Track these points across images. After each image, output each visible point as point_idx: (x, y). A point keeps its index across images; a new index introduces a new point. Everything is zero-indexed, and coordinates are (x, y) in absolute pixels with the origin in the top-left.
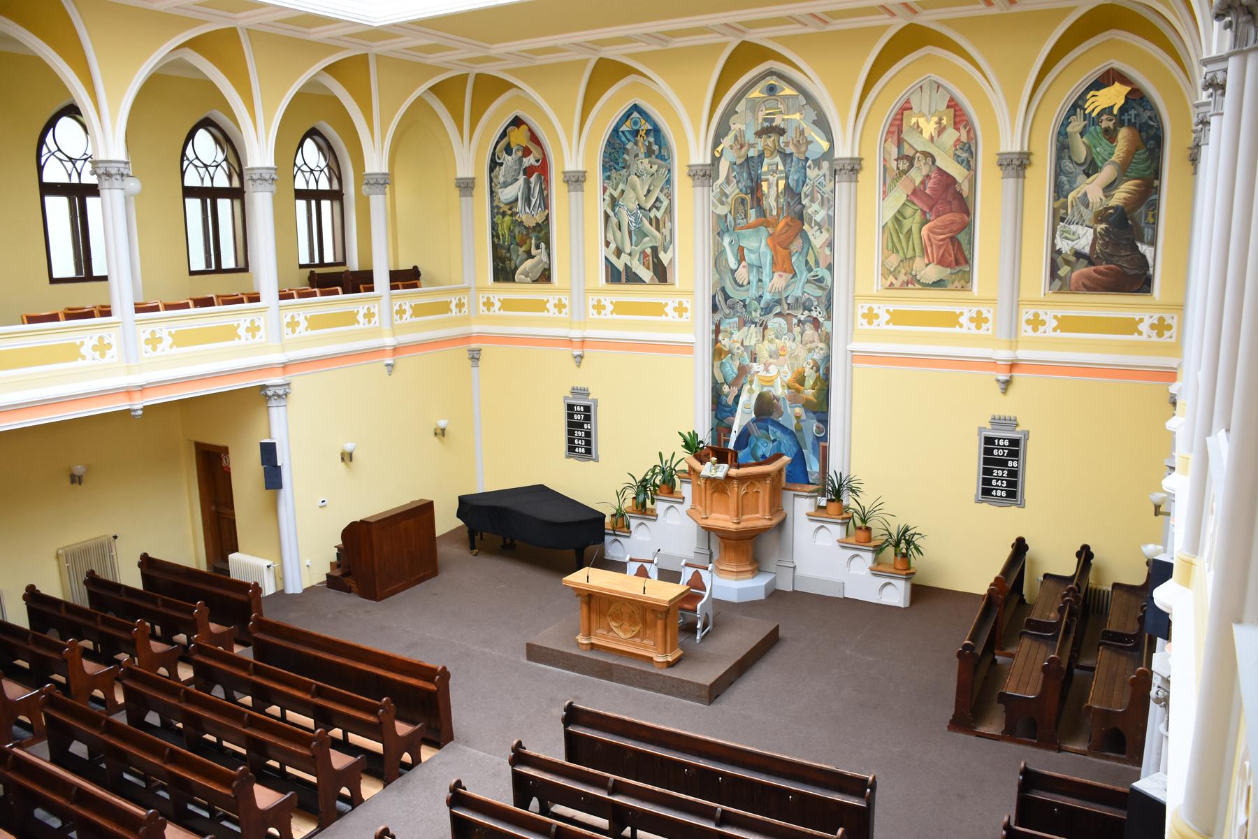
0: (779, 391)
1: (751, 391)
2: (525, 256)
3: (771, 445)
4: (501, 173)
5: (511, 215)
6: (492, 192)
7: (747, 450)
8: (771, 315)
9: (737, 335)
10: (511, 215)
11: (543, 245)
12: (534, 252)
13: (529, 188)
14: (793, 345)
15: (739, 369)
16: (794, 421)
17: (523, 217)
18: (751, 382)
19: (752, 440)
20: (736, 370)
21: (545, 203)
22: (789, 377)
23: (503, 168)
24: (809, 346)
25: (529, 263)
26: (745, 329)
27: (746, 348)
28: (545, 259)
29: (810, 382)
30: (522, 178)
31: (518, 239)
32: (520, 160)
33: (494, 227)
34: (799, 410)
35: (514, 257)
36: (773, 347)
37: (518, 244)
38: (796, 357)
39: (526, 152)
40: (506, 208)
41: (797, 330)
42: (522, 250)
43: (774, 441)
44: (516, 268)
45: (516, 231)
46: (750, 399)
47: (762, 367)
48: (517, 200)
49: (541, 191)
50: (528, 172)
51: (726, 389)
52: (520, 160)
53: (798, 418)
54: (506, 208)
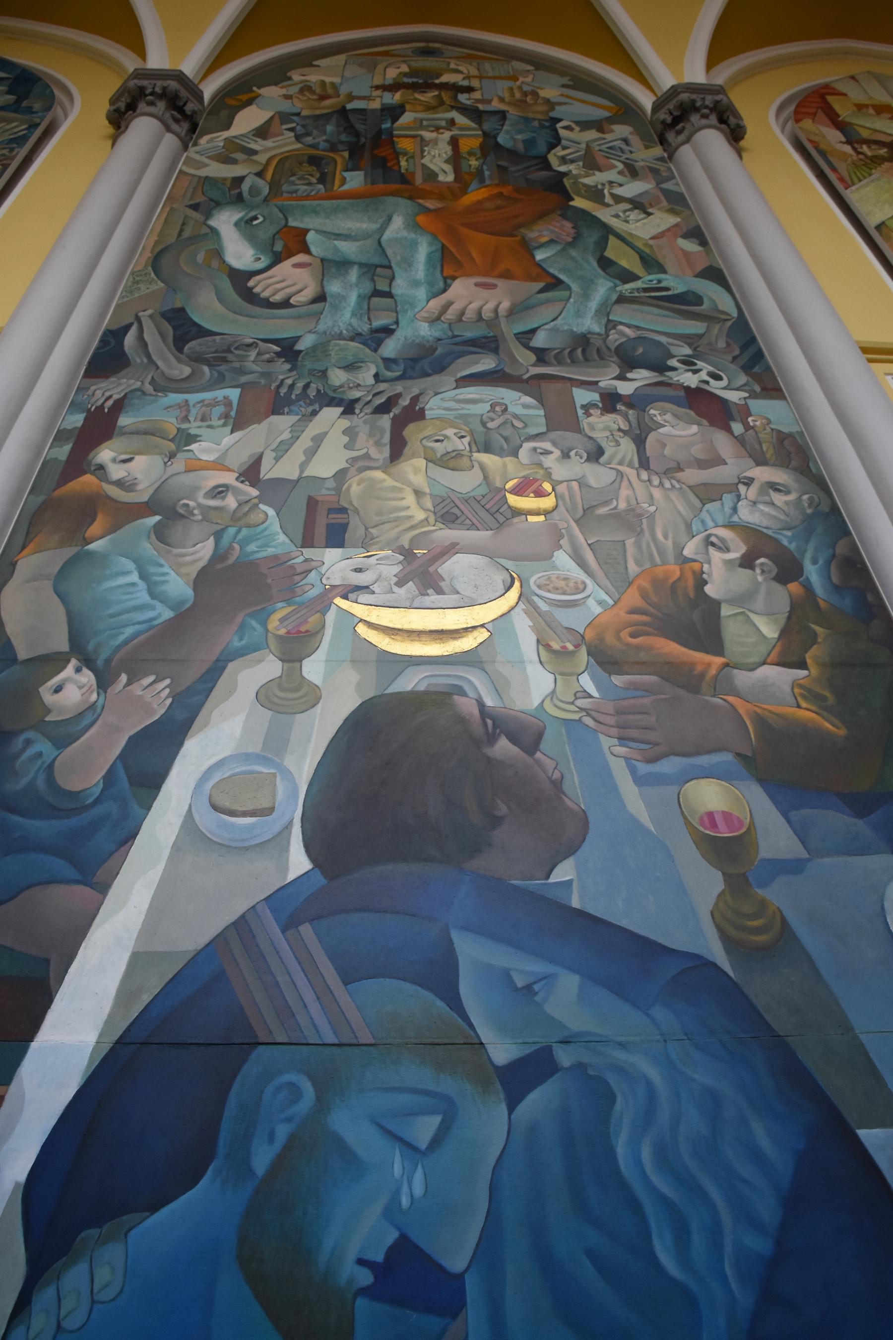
0: (534, 687)
1: (289, 697)
3: (490, 1125)
7: (200, 1209)
8: (447, 380)
9: (217, 445)
14: (598, 476)
15: (203, 580)
16: (706, 884)
18: (296, 646)
19: (273, 1101)
20: (179, 587)
22: (596, 603)
24: (693, 476)
26: (283, 423)
27: (276, 491)
29: (756, 623)
34: (710, 796)
36: (465, 482)
38: (632, 520)
41: (601, 425)
43: (518, 1079)
46: (275, 745)
47: (383, 565)
51: (71, 689)
53: (727, 849)
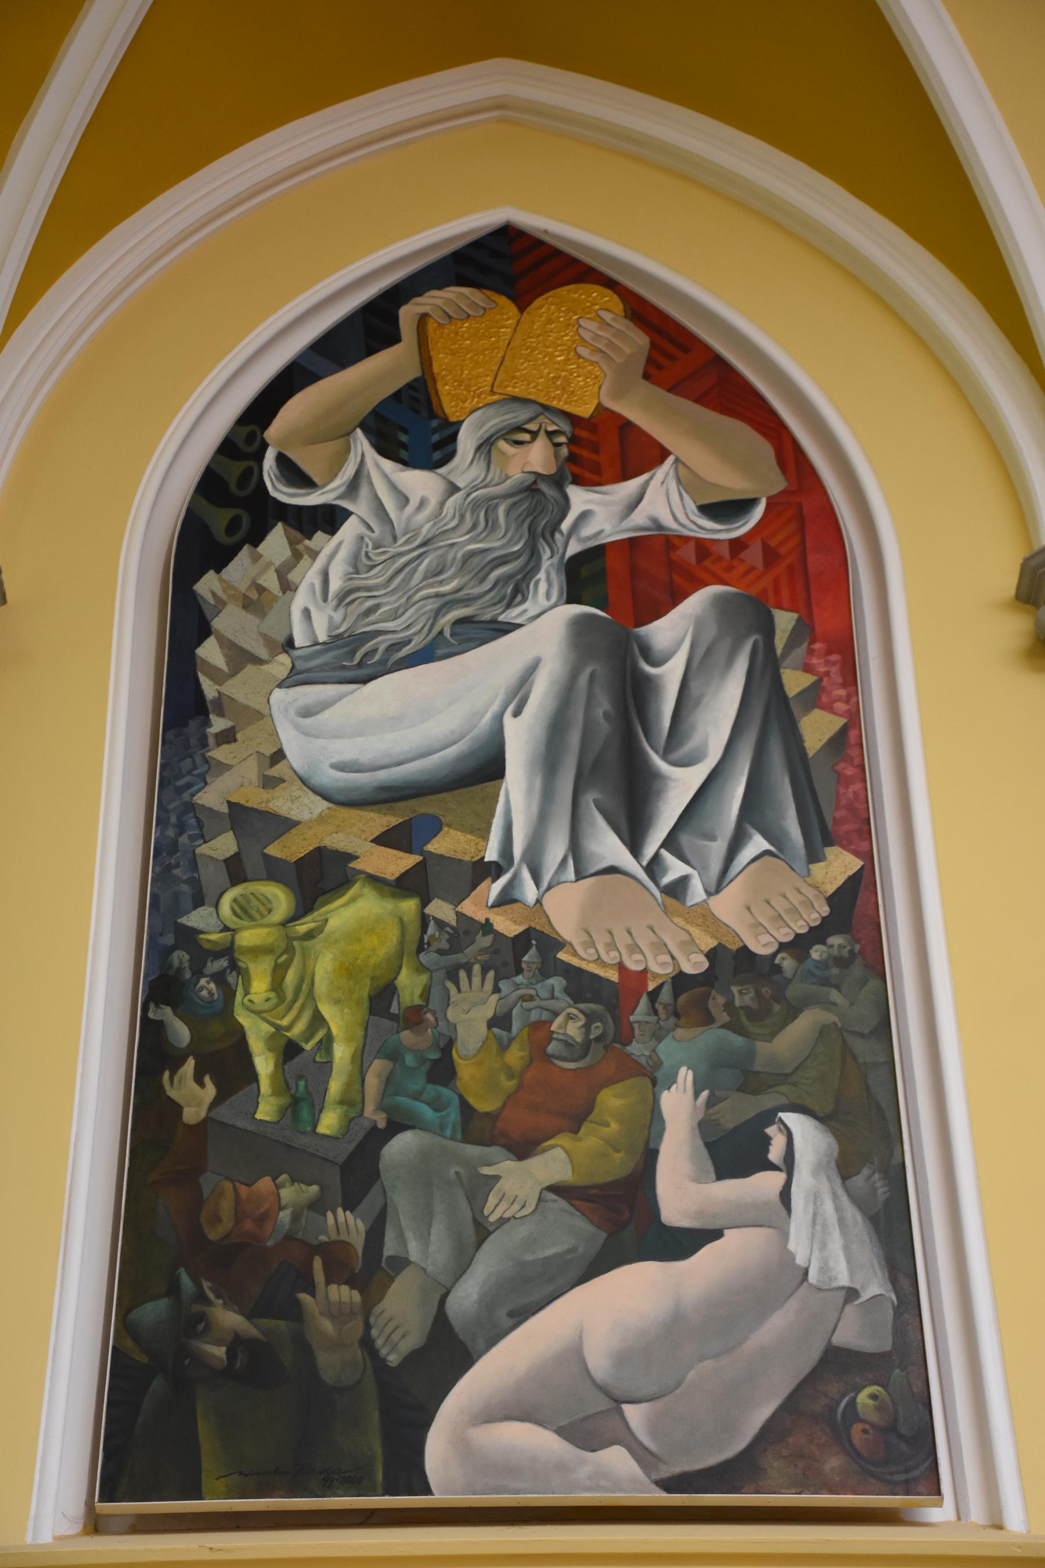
2: (572, 1232)
4: (312, 591)
5: (413, 884)
6: (185, 712)
10: (413, 884)
11: (805, 1136)
12: (681, 1189)
13: (633, 692)
17: (566, 910)
21: (819, 785)
23: (336, 550)
25: (630, 1296)
28: (824, 1238)
30: (545, 630)
31: (482, 1077)
32: (538, 505)
33: (178, 990)
35: (422, 1244)
37: (476, 1128)
39: (606, 450)
40: (355, 835)
42: (520, 1183)
44: (448, 1352)
45: (470, 1012)
48: (487, 767)
49: (769, 712)
50: (623, 583)
52: (538, 505)
54: (355, 835)
